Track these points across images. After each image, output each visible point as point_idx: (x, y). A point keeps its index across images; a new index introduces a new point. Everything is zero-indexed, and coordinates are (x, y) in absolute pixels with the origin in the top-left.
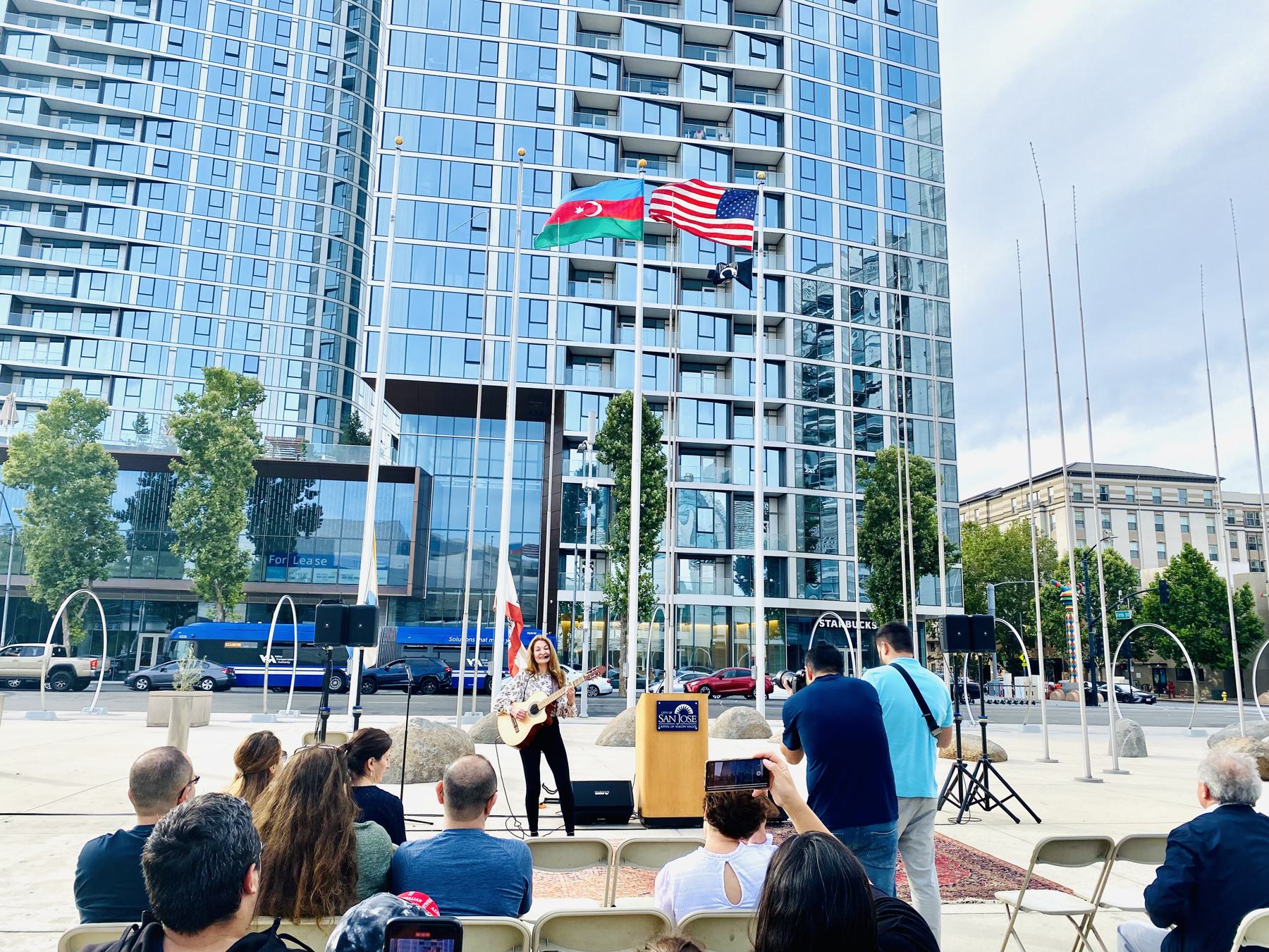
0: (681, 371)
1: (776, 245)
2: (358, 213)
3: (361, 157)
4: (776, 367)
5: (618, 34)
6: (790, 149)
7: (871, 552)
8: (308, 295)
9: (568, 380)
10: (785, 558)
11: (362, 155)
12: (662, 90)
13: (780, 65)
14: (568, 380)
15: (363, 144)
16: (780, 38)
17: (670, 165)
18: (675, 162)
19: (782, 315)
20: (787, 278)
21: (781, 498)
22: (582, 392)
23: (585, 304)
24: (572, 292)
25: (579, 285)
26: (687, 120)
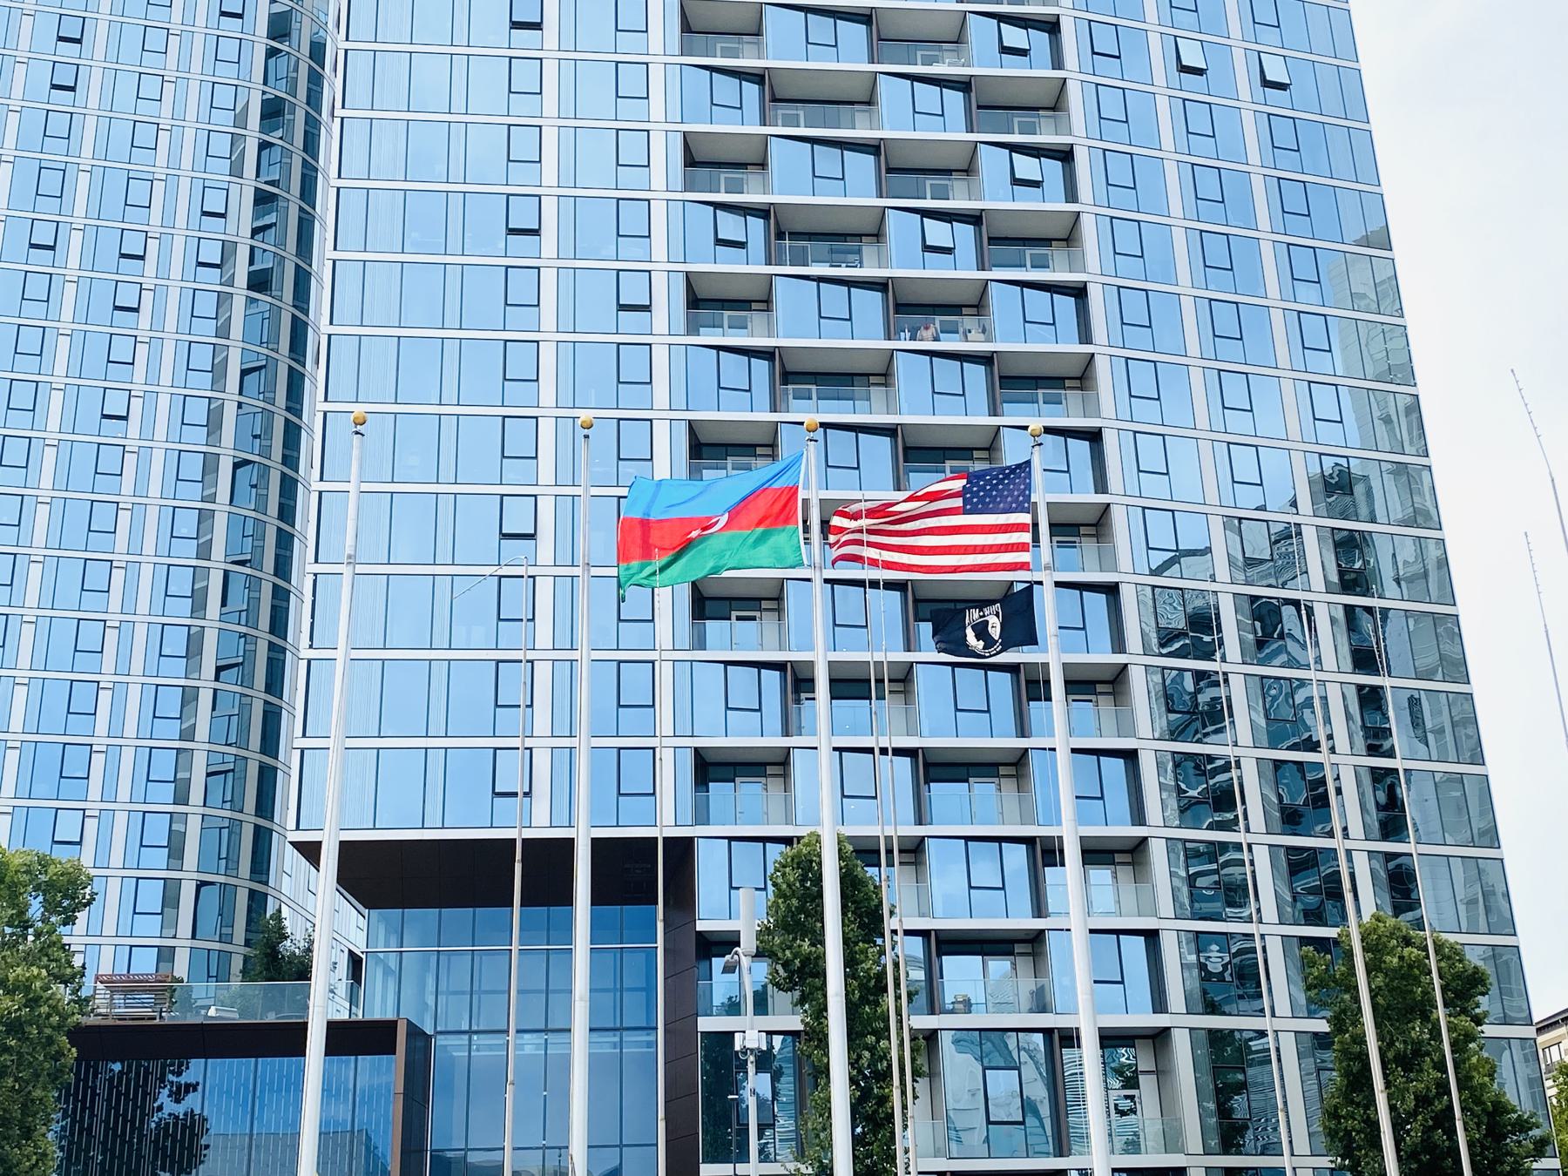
0: (927, 782)
1: (1080, 378)
2: (284, 463)
3: (292, 309)
4: (1101, 598)
5: (758, 33)
6: (1101, 346)
7: (1359, 1148)
8: (204, 449)
9: (702, 815)
10: (1185, 1168)
11: (294, 306)
12: (851, 257)
13: (1058, 63)
14: (702, 817)
15: (296, 284)
16: (1054, 20)
17: (877, 393)
18: (886, 385)
19: (1120, 659)
20: (1123, 589)
21: (1135, 852)
22: (731, 839)
23: (727, 663)
24: (700, 643)
25: (712, 626)
26: (902, 307)
